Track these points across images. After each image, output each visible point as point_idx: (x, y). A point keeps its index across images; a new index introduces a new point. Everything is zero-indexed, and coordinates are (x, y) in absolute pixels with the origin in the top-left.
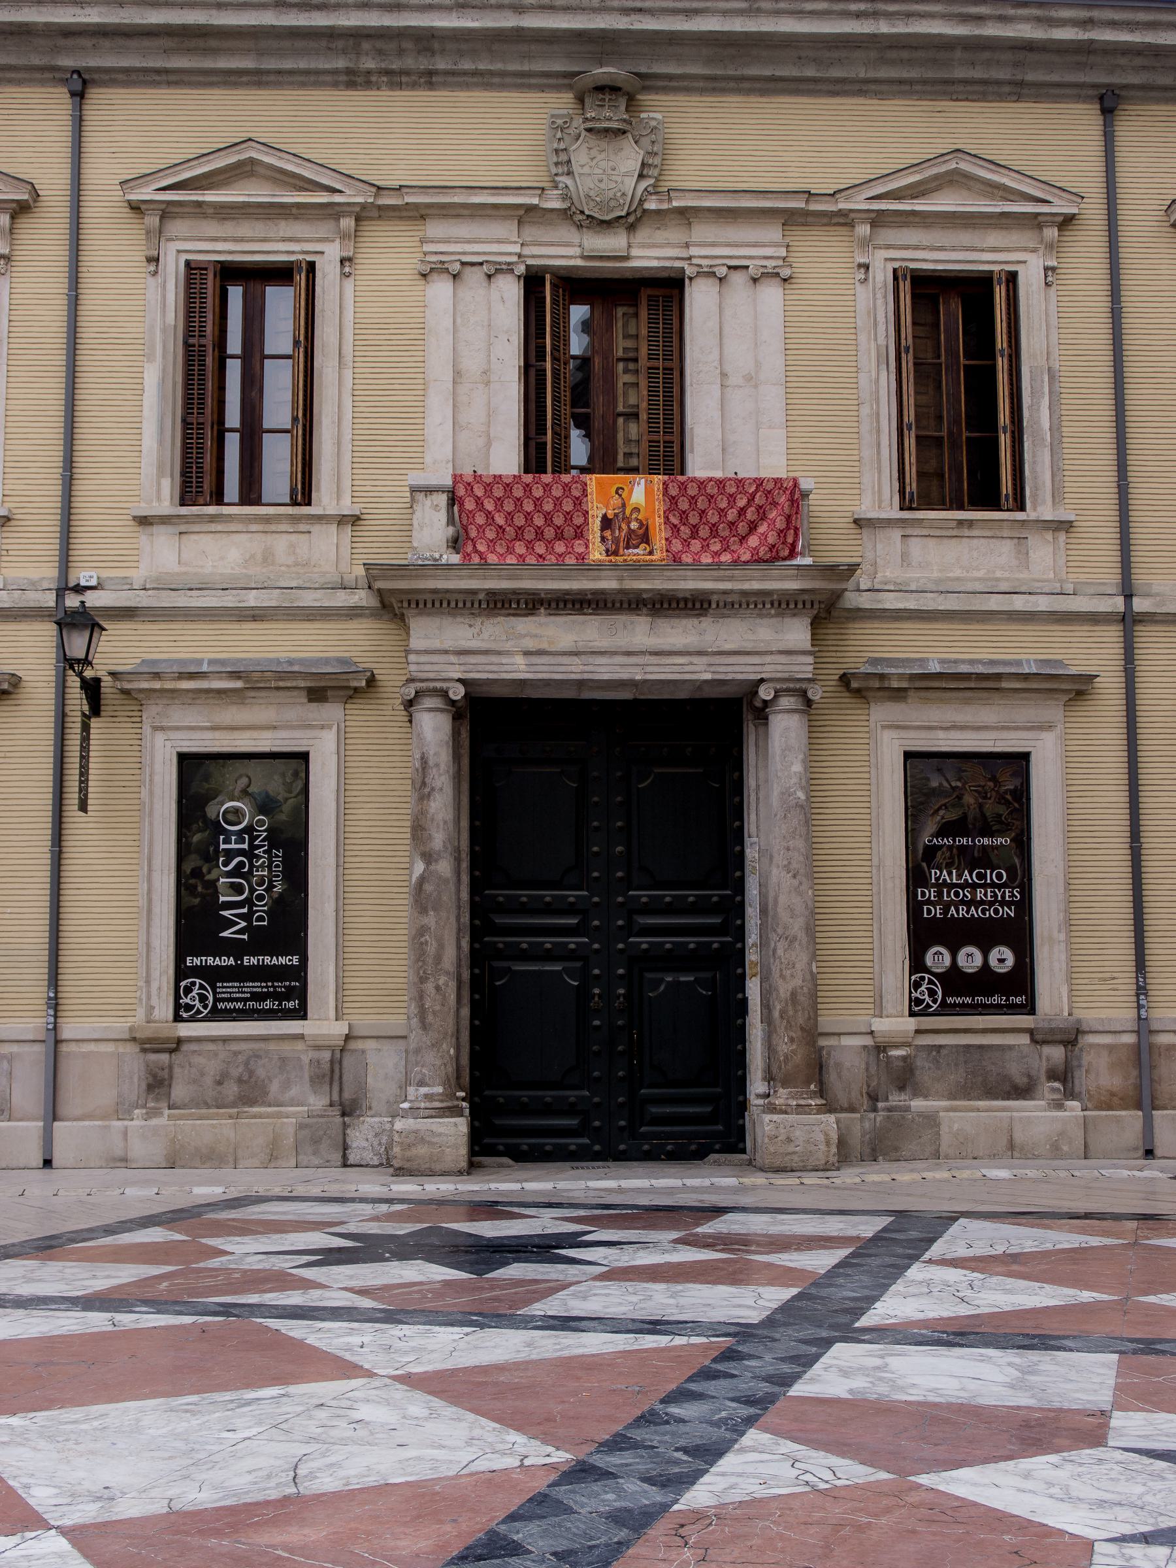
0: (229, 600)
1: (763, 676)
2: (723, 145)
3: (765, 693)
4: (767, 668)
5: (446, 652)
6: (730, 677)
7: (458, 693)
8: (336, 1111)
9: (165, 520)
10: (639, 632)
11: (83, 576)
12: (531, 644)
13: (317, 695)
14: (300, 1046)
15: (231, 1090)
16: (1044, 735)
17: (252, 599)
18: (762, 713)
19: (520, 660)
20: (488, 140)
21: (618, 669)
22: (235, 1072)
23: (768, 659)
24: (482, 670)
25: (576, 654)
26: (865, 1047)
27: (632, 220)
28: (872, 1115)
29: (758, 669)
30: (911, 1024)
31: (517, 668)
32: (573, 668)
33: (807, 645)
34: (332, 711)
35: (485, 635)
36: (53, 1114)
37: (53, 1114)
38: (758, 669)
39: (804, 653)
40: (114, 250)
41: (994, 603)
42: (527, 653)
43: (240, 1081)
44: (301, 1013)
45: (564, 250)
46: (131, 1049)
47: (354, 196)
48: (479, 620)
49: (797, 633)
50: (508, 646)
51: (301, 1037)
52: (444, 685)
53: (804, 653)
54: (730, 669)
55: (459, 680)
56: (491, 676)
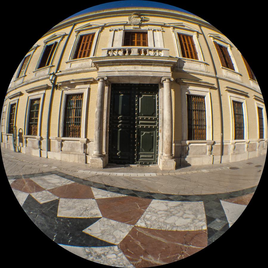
1: (163, 76)
3: (163, 79)
4: (163, 75)
5: (104, 72)
6: (156, 76)
7: (106, 78)
8: (84, 154)
10: (139, 68)
12: (119, 70)
14: (79, 142)
16: (207, 93)
17: (78, 70)
18: (162, 85)
19: (117, 72)
21: (135, 74)
23: (164, 73)
24: (110, 74)
25: (128, 71)
26: (179, 146)
27: (140, 25)
28: (180, 158)
29: (162, 75)
31: (117, 74)
32: (127, 74)
33: (170, 72)
34: (88, 86)
35: (111, 69)
38: (162, 75)
39: (170, 72)
41: (198, 72)
42: (118, 71)
43: (71, 147)
48: (110, 67)
50: (116, 70)
51: (79, 141)
52: (104, 77)
53: (170, 72)
54: (156, 74)
55: (106, 76)
56: (112, 75)
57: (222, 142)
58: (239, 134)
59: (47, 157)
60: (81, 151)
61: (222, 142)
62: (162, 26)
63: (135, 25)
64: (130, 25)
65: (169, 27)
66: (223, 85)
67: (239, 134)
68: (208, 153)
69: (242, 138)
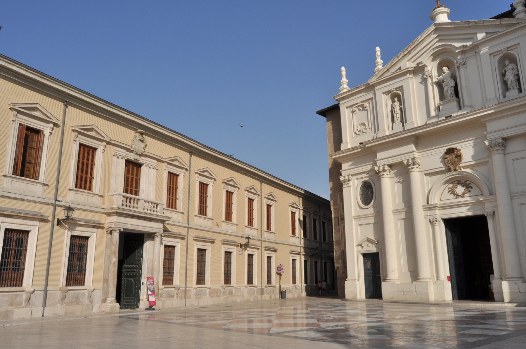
0: (82, 207)
2: (154, 146)
9: (73, 190)
11: (59, 199)
12: (131, 223)
13: (94, 227)
14: (86, 291)
15: (74, 300)
17: (86, 208)
20: (126, 136)
22: (75, 296)
27: (141, 155)
30: (163, 287)
31: (130, 227)
34: (95, 230)
36: (44, 305)
37: (44, 305)
40: (70, 136)
44: (83, 284)
45: (132, 157)
46: (59, 291)
47: (108, 140)
49: (161, 226)
57: (186, 287)
58: (201, 279)
59: (43, 315)
60: (86, 301)
61: (186, 287)
62: (158, 160)
63: (137, 154)
64: (132, 152)
65: (163, 162)
66: (192, 234)
67: (201, 279)
68: (175, 296)
69: (203, 283)
